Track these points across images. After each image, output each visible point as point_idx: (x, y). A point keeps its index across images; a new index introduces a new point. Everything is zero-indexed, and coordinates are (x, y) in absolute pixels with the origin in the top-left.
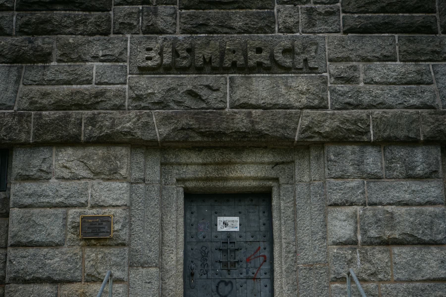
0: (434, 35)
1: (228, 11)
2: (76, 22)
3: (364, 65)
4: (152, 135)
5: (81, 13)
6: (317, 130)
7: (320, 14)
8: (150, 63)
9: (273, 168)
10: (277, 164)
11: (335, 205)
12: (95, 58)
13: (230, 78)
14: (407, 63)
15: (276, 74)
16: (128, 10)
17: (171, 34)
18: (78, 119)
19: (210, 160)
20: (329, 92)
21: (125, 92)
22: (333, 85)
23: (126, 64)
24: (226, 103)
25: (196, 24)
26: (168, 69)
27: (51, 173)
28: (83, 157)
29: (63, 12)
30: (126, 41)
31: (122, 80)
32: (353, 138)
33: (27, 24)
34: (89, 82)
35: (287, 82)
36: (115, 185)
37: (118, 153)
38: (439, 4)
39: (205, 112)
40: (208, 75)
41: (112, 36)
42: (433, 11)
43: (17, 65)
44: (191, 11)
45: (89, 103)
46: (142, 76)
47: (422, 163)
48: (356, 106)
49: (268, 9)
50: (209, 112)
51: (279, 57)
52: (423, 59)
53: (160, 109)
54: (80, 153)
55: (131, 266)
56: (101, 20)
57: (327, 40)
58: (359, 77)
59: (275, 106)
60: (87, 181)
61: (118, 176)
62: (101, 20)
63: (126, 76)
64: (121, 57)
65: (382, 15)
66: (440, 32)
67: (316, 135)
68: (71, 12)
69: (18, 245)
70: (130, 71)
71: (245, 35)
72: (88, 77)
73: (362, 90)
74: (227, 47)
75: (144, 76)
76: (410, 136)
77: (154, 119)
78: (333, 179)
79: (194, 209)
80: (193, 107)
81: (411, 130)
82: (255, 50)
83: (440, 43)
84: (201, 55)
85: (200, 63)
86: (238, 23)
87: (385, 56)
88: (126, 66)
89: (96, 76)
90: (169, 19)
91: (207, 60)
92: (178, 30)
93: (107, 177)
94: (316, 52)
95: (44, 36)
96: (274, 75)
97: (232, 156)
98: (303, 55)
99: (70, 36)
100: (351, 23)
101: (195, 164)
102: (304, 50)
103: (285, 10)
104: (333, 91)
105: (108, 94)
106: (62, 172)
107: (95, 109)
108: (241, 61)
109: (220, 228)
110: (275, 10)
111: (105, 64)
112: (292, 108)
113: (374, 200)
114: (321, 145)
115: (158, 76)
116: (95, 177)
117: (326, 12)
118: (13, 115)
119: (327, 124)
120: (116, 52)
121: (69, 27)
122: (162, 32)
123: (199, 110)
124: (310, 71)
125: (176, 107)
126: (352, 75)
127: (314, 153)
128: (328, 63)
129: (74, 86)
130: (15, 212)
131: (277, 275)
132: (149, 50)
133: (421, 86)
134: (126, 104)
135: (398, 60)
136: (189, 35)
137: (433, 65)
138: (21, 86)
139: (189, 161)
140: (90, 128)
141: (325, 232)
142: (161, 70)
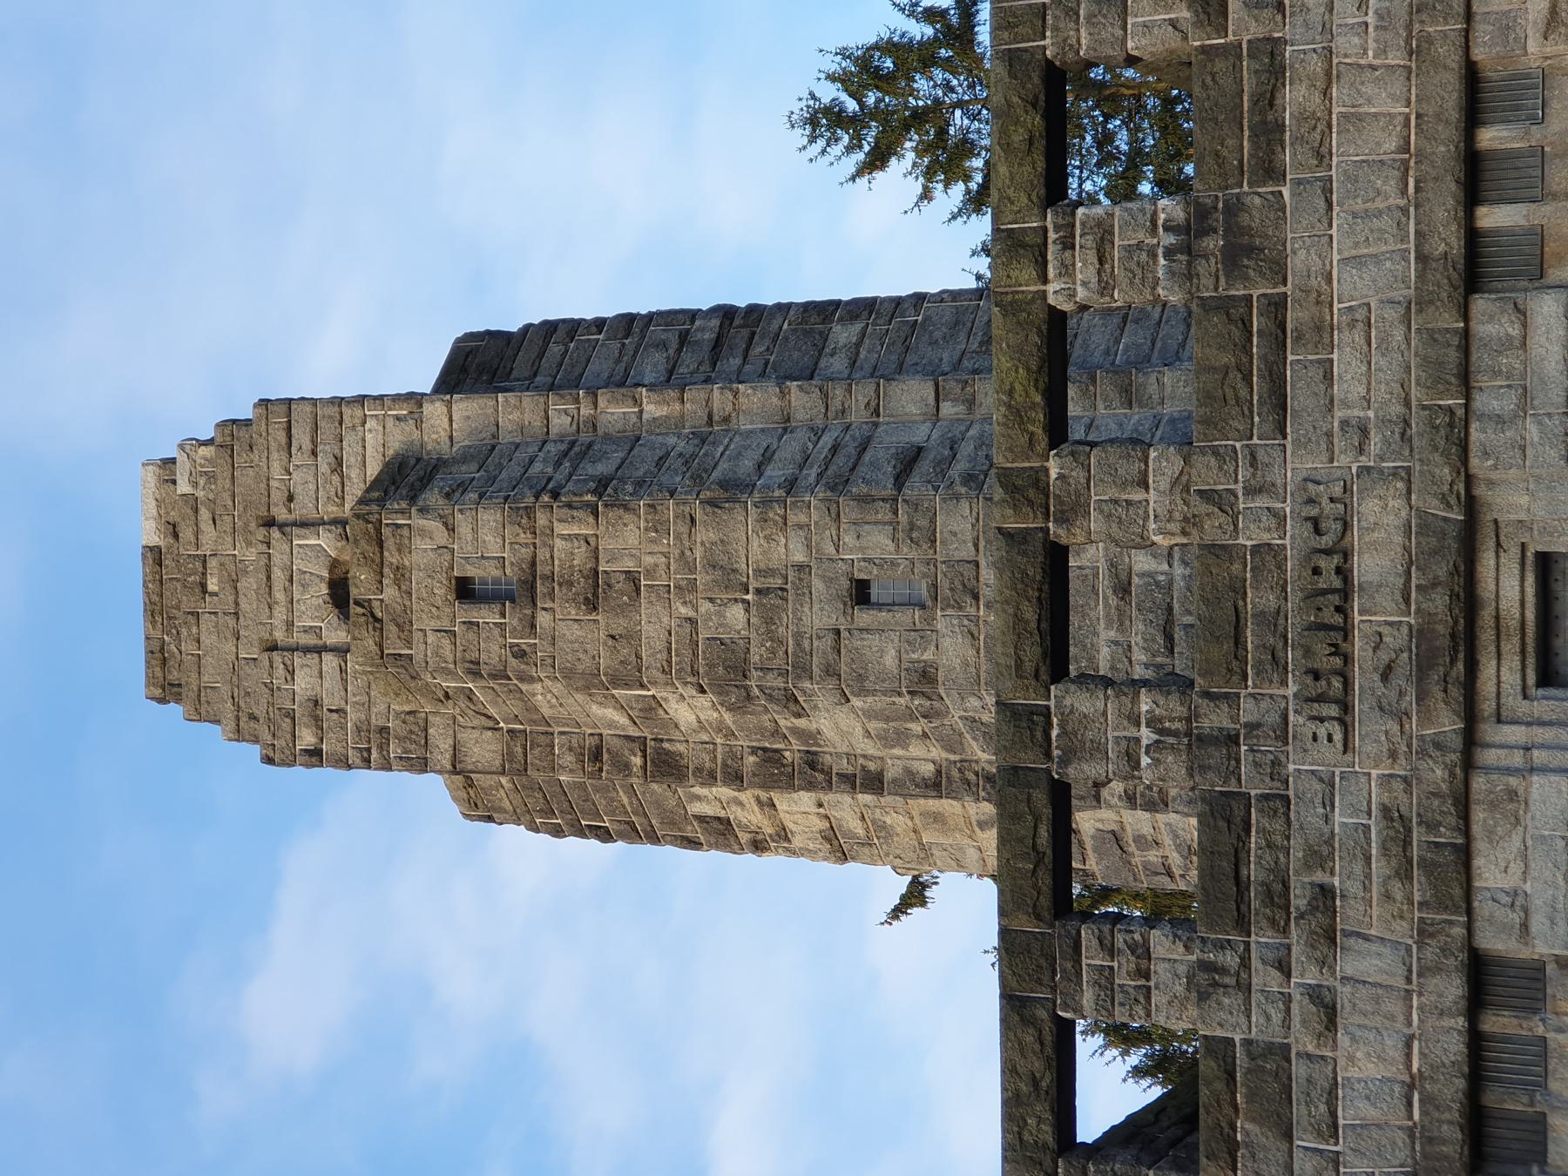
0: (1289, 299)
1: (1249, 616)
2: (1269, 846)
3: (1339, 410)
4: (1454, 736)
5: (1253, 839)
6: (1446, 488)
7: (1254, 475)
8: (1338, 737)
9: (1505, 551)
10: (1498, 545)
13: (1360, 614)
14: (1336, 343)
15: (1353, 545)
16: (1248, 767)
17: (1287, 703)
18: (1429, 847)
19: (1492, 648)
20: (1384, 465)
21: (1384, 775)
22: (1372, 458)
23: (1337, 773)
24: (1401, 622)
25: (1271, 665)
26: (1346, 707)
27: (1516, 891)
28: (1491, 842)
29: (1252, 866)
30: (1299, 771)
31: (1363, 779)
32: (1459, 432)
33: (1273, 922)
34: (1368, 827)
35: (1367, 529)
36: (1535, 793)
37: (1484, 787)
38: (1238, 290)
39: (1417, 655)
40: (1356, 647)
41: (1291, 793)
42: (1249, 298)
43: (1338, 937)
44: (1249, 671)
45: (1401, 829)
46: (1357, 749)
47: (1501, 325)
48: (1407, 423)
49: (1245, 553)
50: (1417, 648)
51: (1326, 541)
52: (1328, 318)
53: (1411, 723)
54: (1480, 845)
56: (1266, 809)
57: (1298, 466)
58: (1358, 417)
59: (1407, 549)
60: (1528, 836)
61: (1521, 792)
62: (1266, 809)
63: (1356, 772)
64: (1326, 779)
65: (1255, 379)
66: (1282, 289)
67: (1456, 487)
68: (1252, 854)
70: (1349, 767)
71: (1289, 590)
72: (1360, 831)
73: (1381, 413)
74: (1312, 618)
75: (1357, 745)
76: (1457, 343)
77: (1428, 732)
78: (1527, 463)
80: (1408, 673)
81: (1448, 342)
82: (1316, 577)
83: (1303, 291)
84: (1324, 659)
86: (1271, 600)
87: (1324, 377)
88: (1341, 772)
89: (1358, 817)
90: (1263, 705)
91: (1333, 650)
92: (1281, 692)
93: (1523, 806)
94: (1319, 483)
95: (1292, 896)
96: (1356, 547)
97: (1486, 616)
98: (1323, 504)
99: (1291, 856)
100: (1268, 427)
101: (1498, 670)
102: (1314, 502)
103: (1248, 528)
104: (1382, 459)
105: (1386, 801)
106: (1514, 874)
107: (1411, 821)
108: (1336, 599)
110: (1249, 543)
111: (1337, 804)
112: (1409, 523)
114: (1469, 480)
115: (1357, 724)
116: (1523, 824)
117: (1252, 466)
118: (1421, 945)
119: (1437, 471)
120: (1318, 786)
121: (1278, 858)
122: (1285, 717)
123: (1414, 663)
124: (1348, 493)
125: (1408, 698)
126: (1356, 430)
127: (1480, 491)
128: (1336, 464)
129: (1374, 852)
132: (1315, 738)
133: (1373, 321)
134: (1402, 773)
135: (1331, 356)
136: (1290, 675)
137: (1339, 303)
138: (1373, 932)
139: (1495, 680)
140: (1442, 829)
142: (1348, 719)
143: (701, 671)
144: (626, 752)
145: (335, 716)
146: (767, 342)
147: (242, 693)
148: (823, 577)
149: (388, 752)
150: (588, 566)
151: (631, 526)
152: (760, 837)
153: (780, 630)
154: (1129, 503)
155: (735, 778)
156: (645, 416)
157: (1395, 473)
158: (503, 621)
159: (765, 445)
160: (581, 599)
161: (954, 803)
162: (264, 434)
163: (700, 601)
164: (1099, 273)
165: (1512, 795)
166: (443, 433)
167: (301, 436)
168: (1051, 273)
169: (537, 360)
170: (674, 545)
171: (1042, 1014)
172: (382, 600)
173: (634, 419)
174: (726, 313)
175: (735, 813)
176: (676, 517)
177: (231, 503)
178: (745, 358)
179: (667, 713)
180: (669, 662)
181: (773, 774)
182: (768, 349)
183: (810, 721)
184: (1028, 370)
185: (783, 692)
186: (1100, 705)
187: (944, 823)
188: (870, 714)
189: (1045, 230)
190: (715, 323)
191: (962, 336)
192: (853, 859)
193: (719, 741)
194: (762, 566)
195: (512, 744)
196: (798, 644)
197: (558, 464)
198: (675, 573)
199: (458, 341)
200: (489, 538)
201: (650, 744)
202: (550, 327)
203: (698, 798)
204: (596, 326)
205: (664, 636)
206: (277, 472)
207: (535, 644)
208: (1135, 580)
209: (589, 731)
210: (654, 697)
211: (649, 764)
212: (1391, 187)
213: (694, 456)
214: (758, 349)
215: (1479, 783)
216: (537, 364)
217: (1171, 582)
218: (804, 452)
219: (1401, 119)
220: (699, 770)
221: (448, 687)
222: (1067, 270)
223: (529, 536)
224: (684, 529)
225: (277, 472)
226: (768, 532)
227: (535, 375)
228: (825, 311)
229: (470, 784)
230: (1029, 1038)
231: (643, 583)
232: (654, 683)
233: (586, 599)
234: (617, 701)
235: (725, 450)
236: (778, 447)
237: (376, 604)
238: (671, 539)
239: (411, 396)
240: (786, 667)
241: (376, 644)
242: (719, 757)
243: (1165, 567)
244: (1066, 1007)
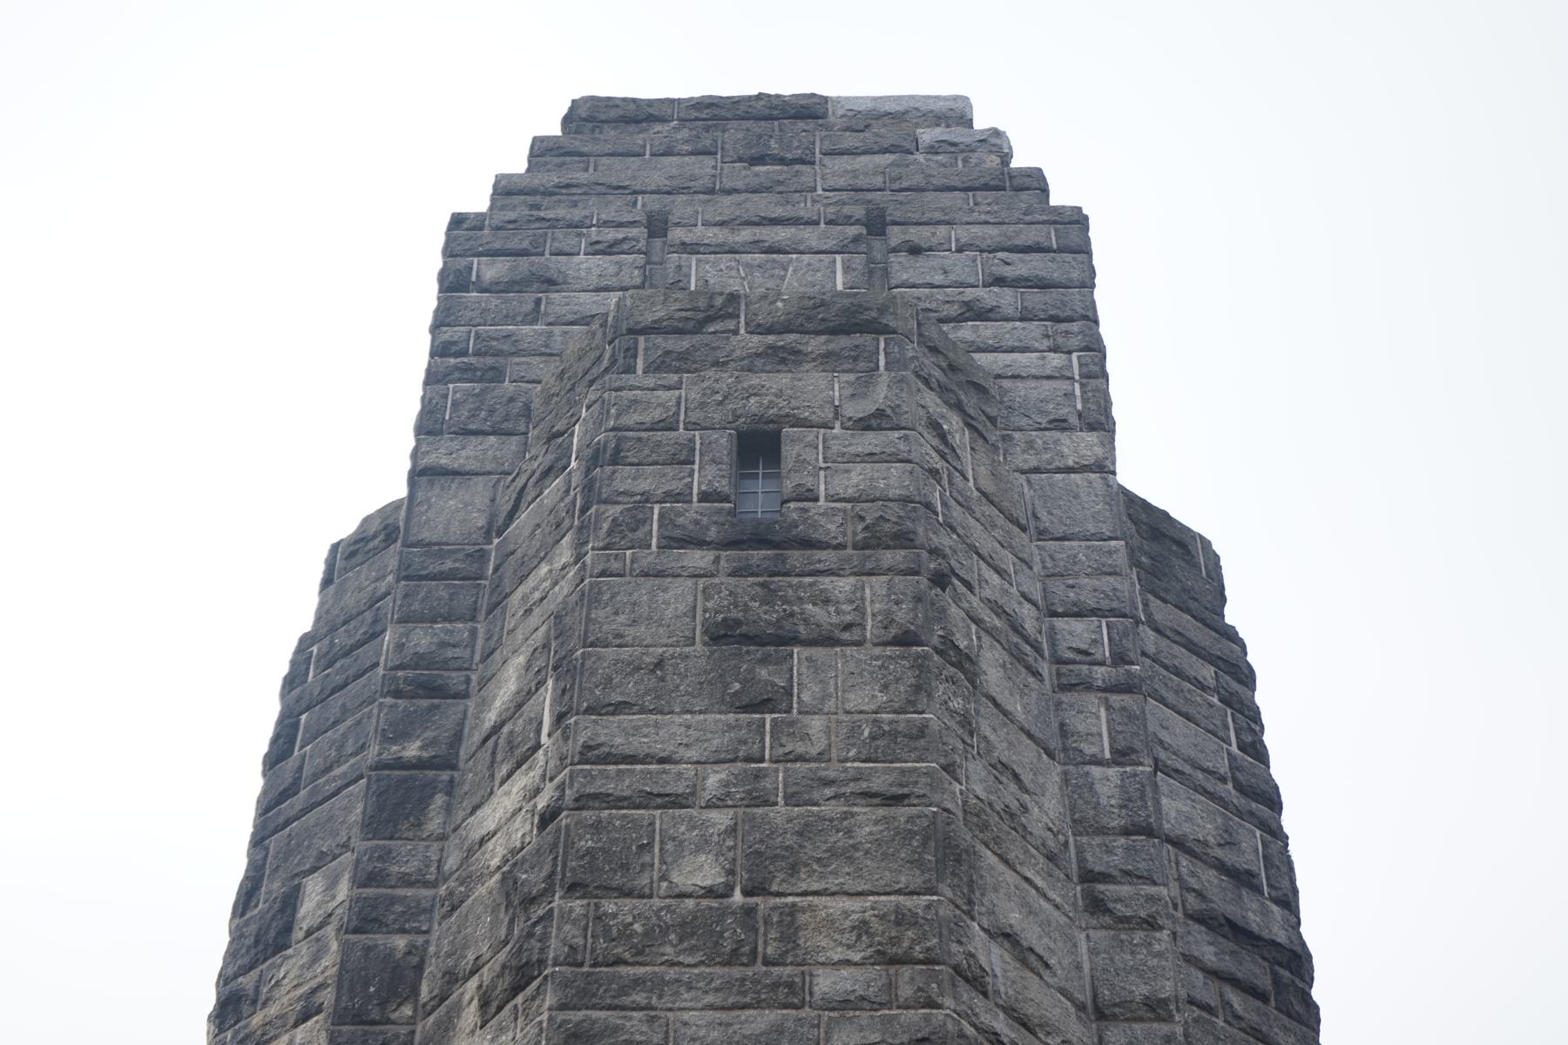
143: (585, 813)
144: (429, 734)
145: (529, 307)
147: (576, 198)
149: (460, 380)
150: (801, 628)
151: (882, 698)
152: (246, 1009)
153: (668, 949)
155: (365, 919)
156: (1096, 771)
158: (695, 499)
159: (1052, 962)
160: (736, 614)
162: (1028, 218)
163: (731, 812)
166: (1047, 456)
167: (1023, 266)
169: (1183, 640)
170: (846, 770)
172: (736, 332)
173: (1089, 749)
174: (1298, 962)
175: (300, 952)
176: (903, 771)
177: (905, 184)
179: (503, 783)
180: (606, 759)
181: (367, 985)
182: (1239, 1018)
183: (473, 1032)
185: (535, 957)
190: (1281, 937)
193: (442, 890)
194: (802, 918)
195: (460, 556)
196: (637, 982)
197: (998, 610)
198: (786, 770)
199: (1206, 544)
200: (855, 478)
201: (445, 776)
203: (332, 885)
204: (1253, 744)
205: (659, 749)
206: (962, 233)
207: (649, 546)
209: (474, 677)
210: (538, 746)
211: (404, 773)
213: (1025, 832)
214: (1236, 1000)
216: (1177, 638)
218: (1041, 1026)
220: (386, 856)
221: (572, 434)
223: (860, 537)
224: (878, 784)
225: (962, 233)
226: (876, 925)
227: (1157, 630)
231: (768, 718)
233: (738, 623)
234: (530, 694)
235: (1037, 888)
236: (1047, 984)
237: (731, 324)
238: (856, 764)
240: (587, 963)
241: (655, 322)
242: (410, 892)
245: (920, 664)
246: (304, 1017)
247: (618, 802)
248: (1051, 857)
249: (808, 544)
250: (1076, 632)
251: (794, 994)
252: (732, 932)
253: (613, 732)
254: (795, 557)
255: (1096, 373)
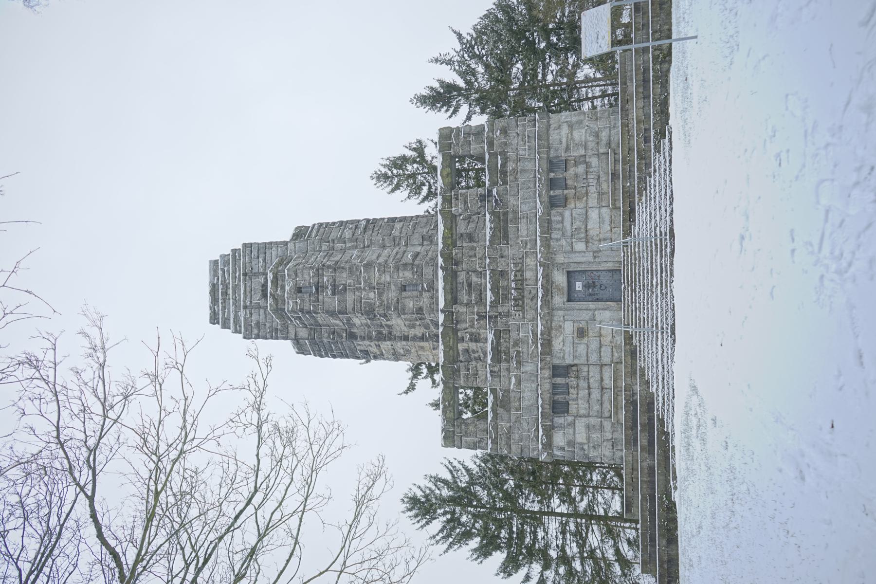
11: (572, 248)
12: (519, 335)
42: (500, 212)
51: (518, 268)
55: (595, 320)
69: (588, 361)
79: (573, 298)
85: (521, 297)
109: (580, 289)
113: (570, 235)
130: (576, 362)
131: (598, 269)
132: (516, 315)
141: (582, 252)
146: (378, 227)
148: (394, 285)
154: (472, 261)
155: (370, 338)
156: (347, 246)
157: (533, 252)
161: (427, 343)
164: (464, 205)
165: (560, 326)
167: (255, 253)
168: (453, 205)
171: (451, 385)
173: (344, 247)
174: (368, 220)
178: (373, 232)
184: (448, 229)
186: (465, 310)
187: (424, 349)
188: (406, 320)
189: (451, 195)
191: (429, 226)
192: (401, 360)
196: (388, 302)
197: (324, 258)
202: (321, 225)
203: (360, 345)
208: (473, 283)
212: (532, 186)
213: (360, 256)
215: (554, 324)
217: (481, 285)
219: (533, 171)
220: (361, 336)
222: (457, 205)
228: (393, 220)
229: (298, 342)
230: (447, 391)
232: (350, 313)
239: (284, 242)
243: (480, 280)
244: (457, 384)
245: (339, 268)
246: (380, 346)
247: (361, 306)
248: (362, 252)
249: (318, 283)
250: (324, 248)
251: (389, 283)
252: (381, 290)
253: (350, 306)
254: (320, 284)
255: (276, 243)
